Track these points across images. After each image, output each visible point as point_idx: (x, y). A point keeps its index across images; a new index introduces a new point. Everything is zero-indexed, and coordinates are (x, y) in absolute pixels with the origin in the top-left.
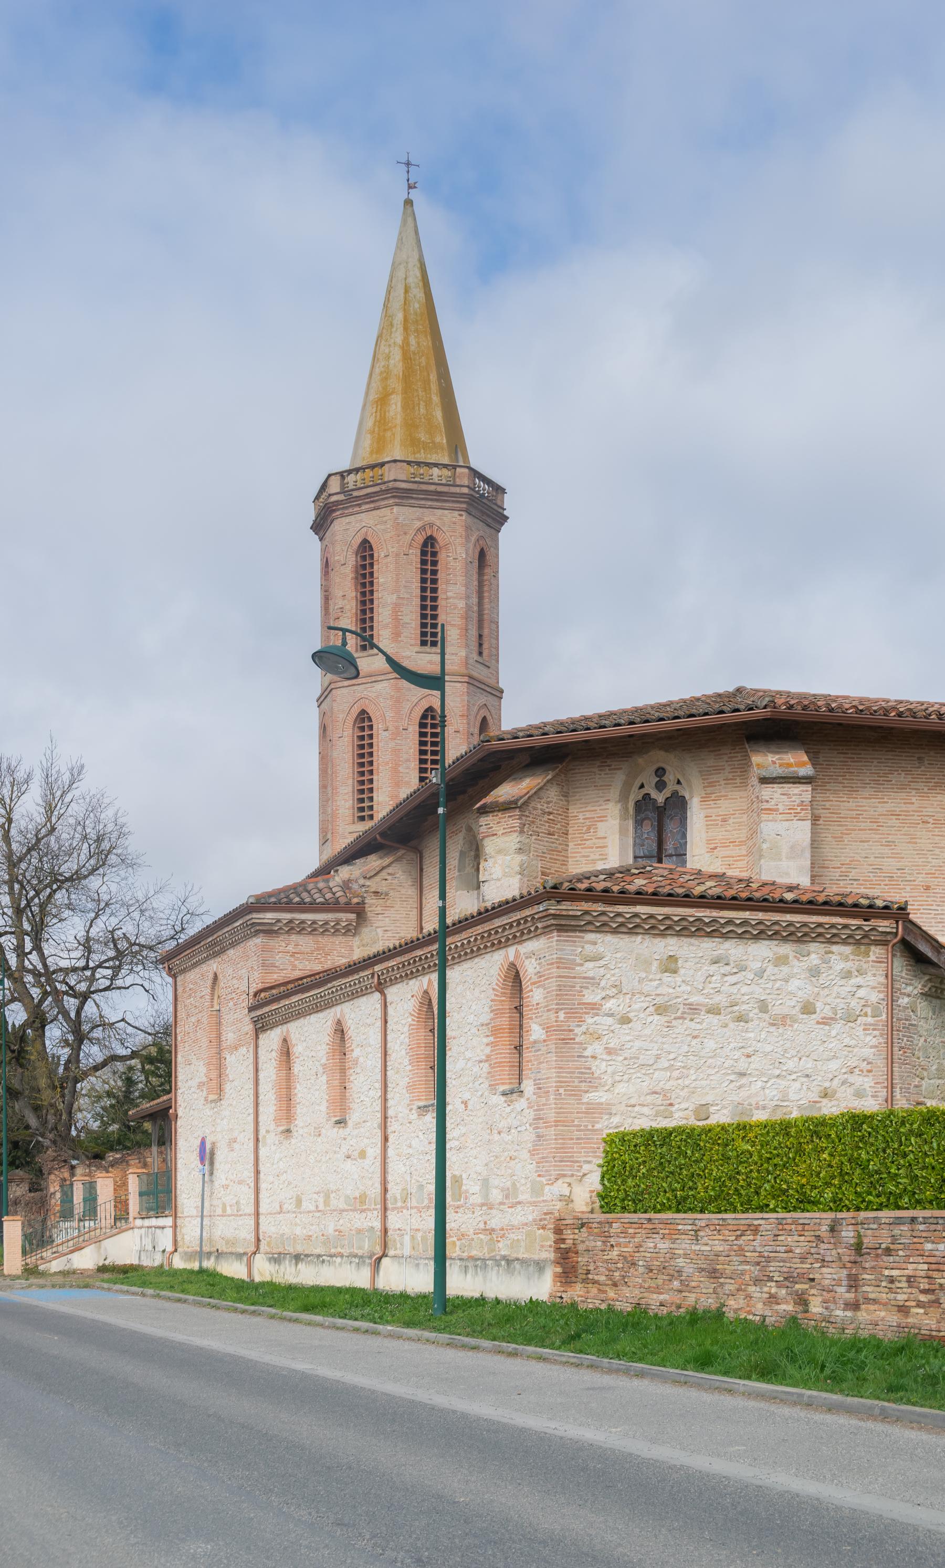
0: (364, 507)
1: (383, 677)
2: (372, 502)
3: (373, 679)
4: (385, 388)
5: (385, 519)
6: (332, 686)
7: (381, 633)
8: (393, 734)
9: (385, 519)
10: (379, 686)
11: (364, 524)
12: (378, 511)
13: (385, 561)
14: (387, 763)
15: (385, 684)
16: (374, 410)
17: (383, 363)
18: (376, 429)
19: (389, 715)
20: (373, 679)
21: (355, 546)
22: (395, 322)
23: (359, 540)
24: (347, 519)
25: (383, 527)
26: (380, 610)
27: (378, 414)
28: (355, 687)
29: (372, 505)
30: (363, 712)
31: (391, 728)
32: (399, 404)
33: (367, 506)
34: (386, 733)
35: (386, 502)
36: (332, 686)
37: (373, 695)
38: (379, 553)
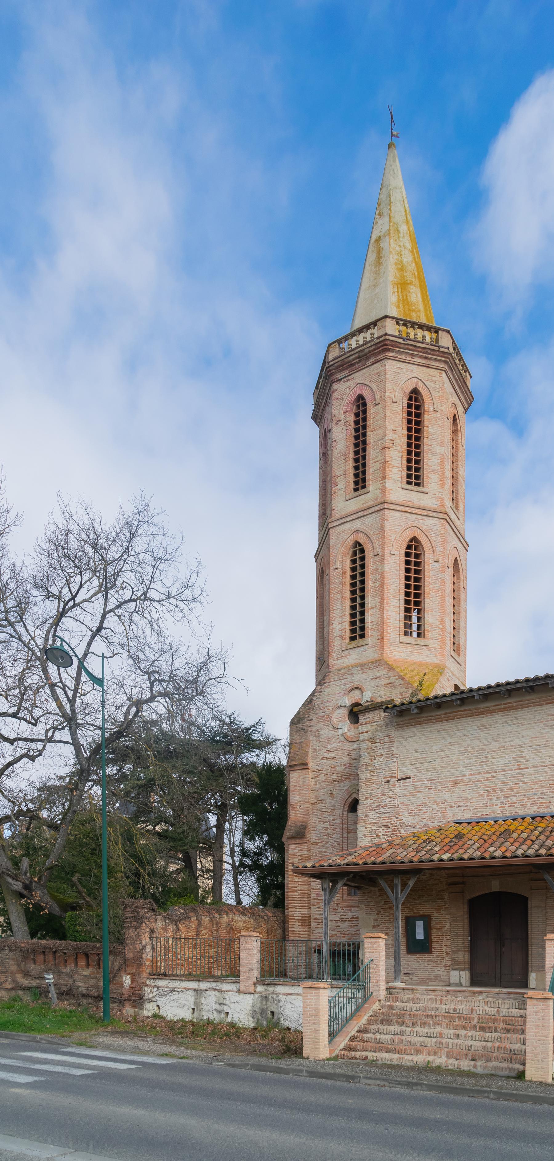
0: (417, 360)
1: (435, 514)
2: (426, 358)
3: (426, 513)
4: (402, 277)
5: (434, 379)
6: (386, 506)
7: (430, 475)
8: (443, 567)
9: (434, 379)
10: (430, 521)
11: (415, 375)
12: (428, 370)
13: (434, 415)
14: (437, 591)
15: (435, 521)
16: (396, 290)
17: (396, 257)
18: (401, 306)
19: (439, 549)
20: (426, 513)
21: (408, 391)
22: (401, 229)
23: (411, 388)
24: (399, 364)
25: (432, 385)
26: (430, 456)
27: (400, 294)
28: (408, 515)
29: (424, 361)
30: (414, 539)
31: (440, 561)
32: (419, 296)
33: (420, 360)
34: (436, 564)
35: (436, 364)
36: (386, 506)
37: (424, 528)
38: (428, 406)
